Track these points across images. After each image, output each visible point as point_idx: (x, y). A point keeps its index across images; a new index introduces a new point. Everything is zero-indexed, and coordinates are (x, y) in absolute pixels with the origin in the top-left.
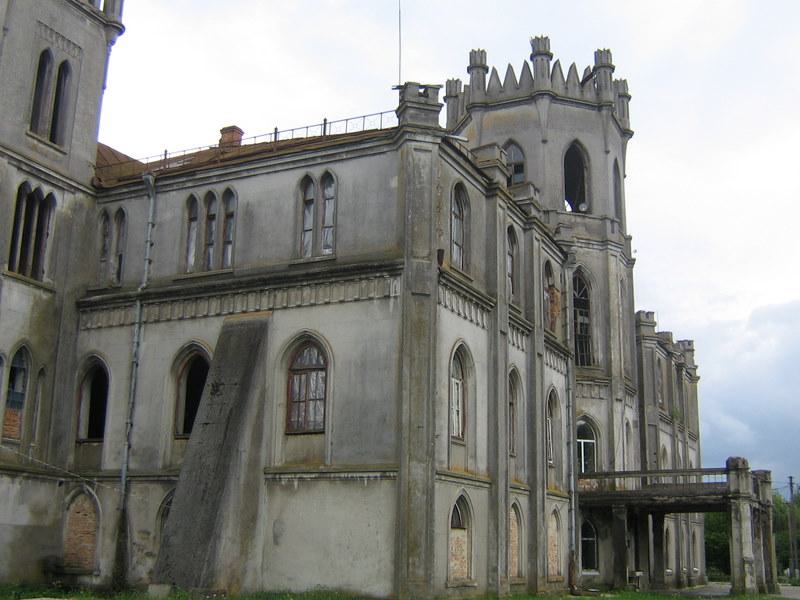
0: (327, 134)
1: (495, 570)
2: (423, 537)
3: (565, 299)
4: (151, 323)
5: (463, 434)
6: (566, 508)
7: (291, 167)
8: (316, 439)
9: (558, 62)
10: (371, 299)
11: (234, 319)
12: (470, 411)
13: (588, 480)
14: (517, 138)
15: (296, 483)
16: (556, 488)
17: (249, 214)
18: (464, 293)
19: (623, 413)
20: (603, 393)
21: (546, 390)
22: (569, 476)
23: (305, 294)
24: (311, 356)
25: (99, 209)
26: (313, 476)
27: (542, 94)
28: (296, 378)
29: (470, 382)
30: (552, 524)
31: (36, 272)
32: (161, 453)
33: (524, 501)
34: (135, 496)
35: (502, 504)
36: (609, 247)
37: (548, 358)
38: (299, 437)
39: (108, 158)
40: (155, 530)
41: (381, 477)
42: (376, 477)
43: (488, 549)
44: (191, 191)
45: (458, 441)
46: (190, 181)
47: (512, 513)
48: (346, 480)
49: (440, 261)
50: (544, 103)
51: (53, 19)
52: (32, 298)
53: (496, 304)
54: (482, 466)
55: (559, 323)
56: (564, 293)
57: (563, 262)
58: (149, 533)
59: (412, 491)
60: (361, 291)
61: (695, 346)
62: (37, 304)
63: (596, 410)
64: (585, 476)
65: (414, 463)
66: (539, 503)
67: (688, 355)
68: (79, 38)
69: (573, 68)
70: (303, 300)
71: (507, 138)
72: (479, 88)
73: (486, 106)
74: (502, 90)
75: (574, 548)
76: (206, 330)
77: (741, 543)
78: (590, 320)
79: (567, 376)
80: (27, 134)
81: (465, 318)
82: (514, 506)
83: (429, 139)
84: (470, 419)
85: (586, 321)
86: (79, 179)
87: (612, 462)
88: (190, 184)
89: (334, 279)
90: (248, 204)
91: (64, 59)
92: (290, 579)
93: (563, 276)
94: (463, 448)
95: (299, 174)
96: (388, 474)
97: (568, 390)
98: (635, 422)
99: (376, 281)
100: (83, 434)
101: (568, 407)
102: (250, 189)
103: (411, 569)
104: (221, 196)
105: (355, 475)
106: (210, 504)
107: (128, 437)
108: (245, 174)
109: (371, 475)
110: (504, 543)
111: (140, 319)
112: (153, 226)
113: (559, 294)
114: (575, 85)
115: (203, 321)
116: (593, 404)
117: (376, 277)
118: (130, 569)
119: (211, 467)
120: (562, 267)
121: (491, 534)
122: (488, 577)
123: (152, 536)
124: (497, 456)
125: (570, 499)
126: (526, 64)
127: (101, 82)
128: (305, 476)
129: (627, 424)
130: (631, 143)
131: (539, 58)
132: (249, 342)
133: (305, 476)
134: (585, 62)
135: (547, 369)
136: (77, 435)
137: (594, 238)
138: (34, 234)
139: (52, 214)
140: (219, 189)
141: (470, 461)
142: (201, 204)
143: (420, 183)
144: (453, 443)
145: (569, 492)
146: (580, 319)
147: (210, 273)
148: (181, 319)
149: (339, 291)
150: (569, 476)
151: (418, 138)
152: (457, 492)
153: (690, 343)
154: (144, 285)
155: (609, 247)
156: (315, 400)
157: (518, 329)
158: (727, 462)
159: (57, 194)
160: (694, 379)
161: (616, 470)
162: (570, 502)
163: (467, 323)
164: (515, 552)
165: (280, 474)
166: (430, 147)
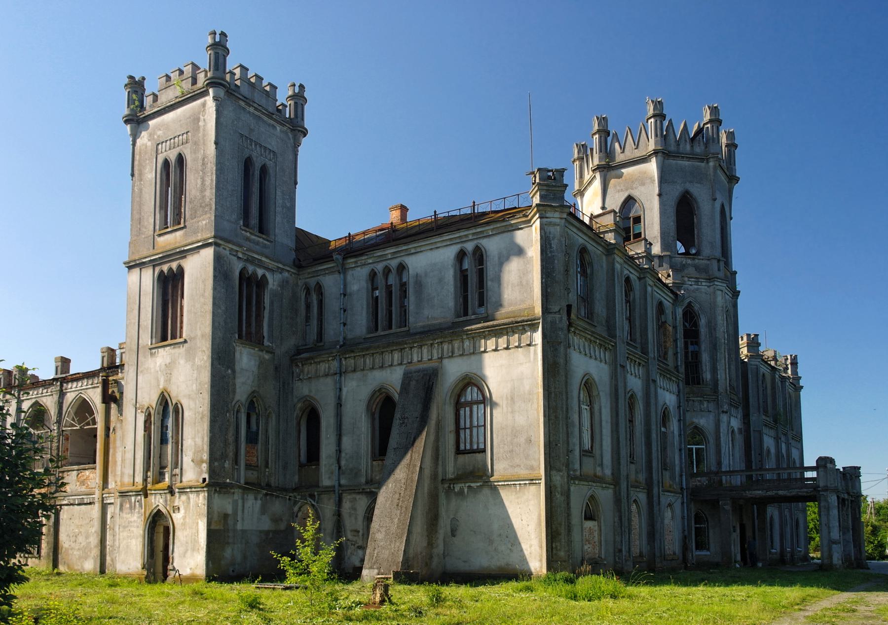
0: (476, 211)
1: (620, 551)
2: (563, 527)
3: (676, 333)
4: (349, 372)
5: (592, 447)
6: (679, 501)
11: (413, 368)
12: (597, 431)
19: (729, 423)
20: (712, 406)
21: (660, 408)
22: (681, 476)
23: (465, 346)
24: (471, 394)
25: (300, 283)
26: (478, 484)
28: (462, 412)
29: (596, 407)
30: (668, 514)
32: (363, 472)
33: (642, 497)
34: (346, 505)
35: (624, 501)
38: (466, 455)
39: (304, 239)
40: (363, 529)
43: (614, 535)
44: (372, 266)
45: (587, 453)
47: (634, 507)
51: (251, 130)
52: (258, 358)
53: (615, 343)
54: (608, 472)
55: (670, 353)
56: (675, 327)
57: (674, 301)
58: (358, 532)
59: (553, 493)
62: (262, 363)
63: (705, 422)
64: (698, 474)
66: (655, 499)
68: (273, 144)
70: (464, 349)
75: (686, 533)
77: (829, 527)
78: (700, 347)
79: (678, 396)
81: (591, 357)
82: (635, 501)
84: (597, 437)
87: (719, 464)
90: (417, 274)
92: (465, 562)
93: (674, 313)
94: (592, 459)
97: (679, 407)
98: (740, 430)
100: (303, 458)
101: (679, 420)
103: (554, 552)
104: (395, 269)
106: (404, 509)
107: (338, 461)
111: (340, 371)
112: (345, 295)
113: (671, 329)
115: (388, 371)
118: (346, 558)
119: (403, 481)
120: (673, 304)
121: (616, 524)
122: (615, 556)
123: (361, 534)
124: (619, 463)
125: (683, 495)
127: (293, 179)
129: (733, 431)
135: (660, 391)
136: (299, 461)
138: (254, 309)
139: (266, 291)
140: (394, 263)
141: (598, 469)
142: (380, 277)
145: (682, 489)
148: (373, 368)
150: (681, 476)
154: (342, 343)
156: (478, 426)
157: (635, 361)
158: (817, 461)
159: (269, 276)
161: (723, 470)
162: (683, 497)
163: (593, 361)
164: (637, 537)
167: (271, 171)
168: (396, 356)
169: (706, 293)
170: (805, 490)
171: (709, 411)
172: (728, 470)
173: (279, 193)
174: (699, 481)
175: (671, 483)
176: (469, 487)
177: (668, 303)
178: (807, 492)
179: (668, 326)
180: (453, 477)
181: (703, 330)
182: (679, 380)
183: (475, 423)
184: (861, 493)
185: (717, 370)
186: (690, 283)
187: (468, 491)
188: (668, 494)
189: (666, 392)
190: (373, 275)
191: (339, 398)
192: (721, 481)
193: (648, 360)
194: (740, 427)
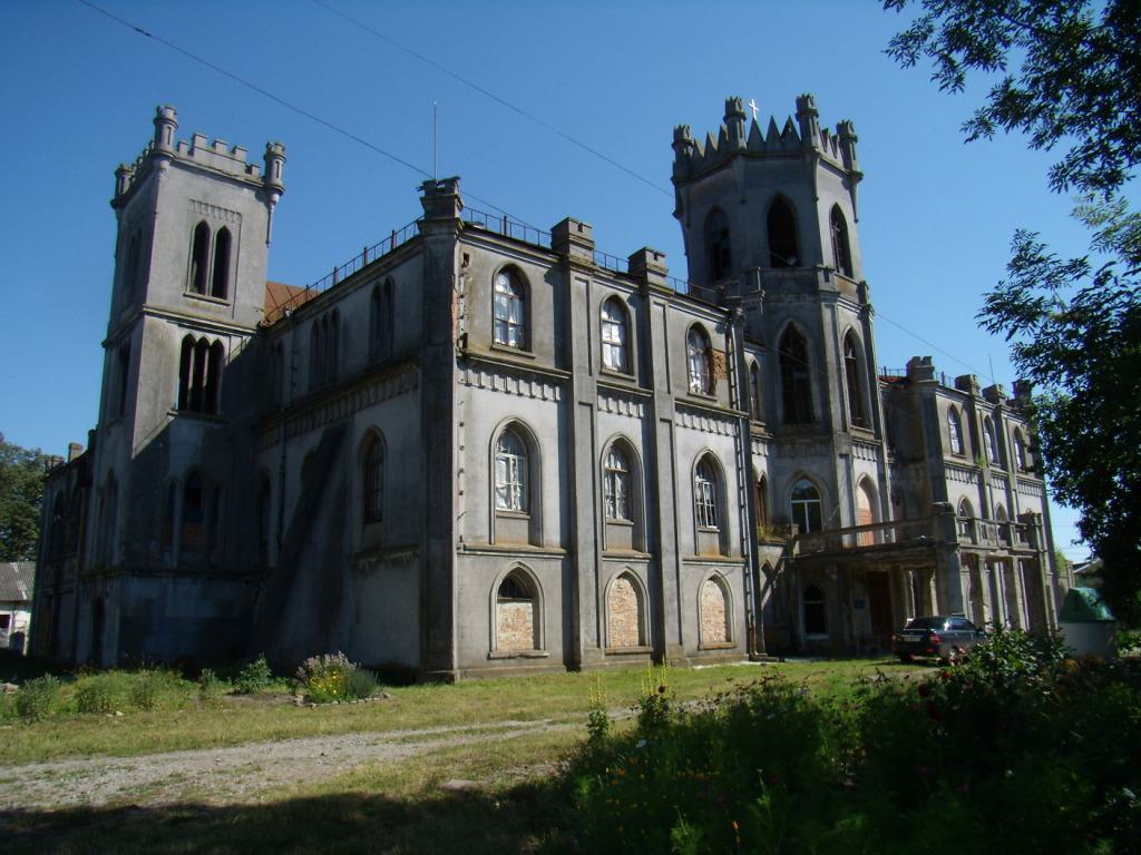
9: (754, 122)
10: (407, 391)
19: (849, 468)
27: (735, 155)
31: (211, 408)
33: (642, 571)
37: (678, 418)
48: (395, 562)
49: (465, 345)
50: (738, 165)
53: (571, 376)
69: (773, 125)
76: (314, 439)
80: (185, 295)
85: (804, 376)
86: (246, 324)
91: (222, 226)
126: (722, 132)
132: (336, 439)
134: (785, 113)
140: (330, 311)
144: (498, 517)
146: (797, 375)
152: (507, 566)
159: (224, 340)
167: (234, 234)
173: (242, 254)
186: (788, 300)
190: (315, 326)
191: (283, 467)
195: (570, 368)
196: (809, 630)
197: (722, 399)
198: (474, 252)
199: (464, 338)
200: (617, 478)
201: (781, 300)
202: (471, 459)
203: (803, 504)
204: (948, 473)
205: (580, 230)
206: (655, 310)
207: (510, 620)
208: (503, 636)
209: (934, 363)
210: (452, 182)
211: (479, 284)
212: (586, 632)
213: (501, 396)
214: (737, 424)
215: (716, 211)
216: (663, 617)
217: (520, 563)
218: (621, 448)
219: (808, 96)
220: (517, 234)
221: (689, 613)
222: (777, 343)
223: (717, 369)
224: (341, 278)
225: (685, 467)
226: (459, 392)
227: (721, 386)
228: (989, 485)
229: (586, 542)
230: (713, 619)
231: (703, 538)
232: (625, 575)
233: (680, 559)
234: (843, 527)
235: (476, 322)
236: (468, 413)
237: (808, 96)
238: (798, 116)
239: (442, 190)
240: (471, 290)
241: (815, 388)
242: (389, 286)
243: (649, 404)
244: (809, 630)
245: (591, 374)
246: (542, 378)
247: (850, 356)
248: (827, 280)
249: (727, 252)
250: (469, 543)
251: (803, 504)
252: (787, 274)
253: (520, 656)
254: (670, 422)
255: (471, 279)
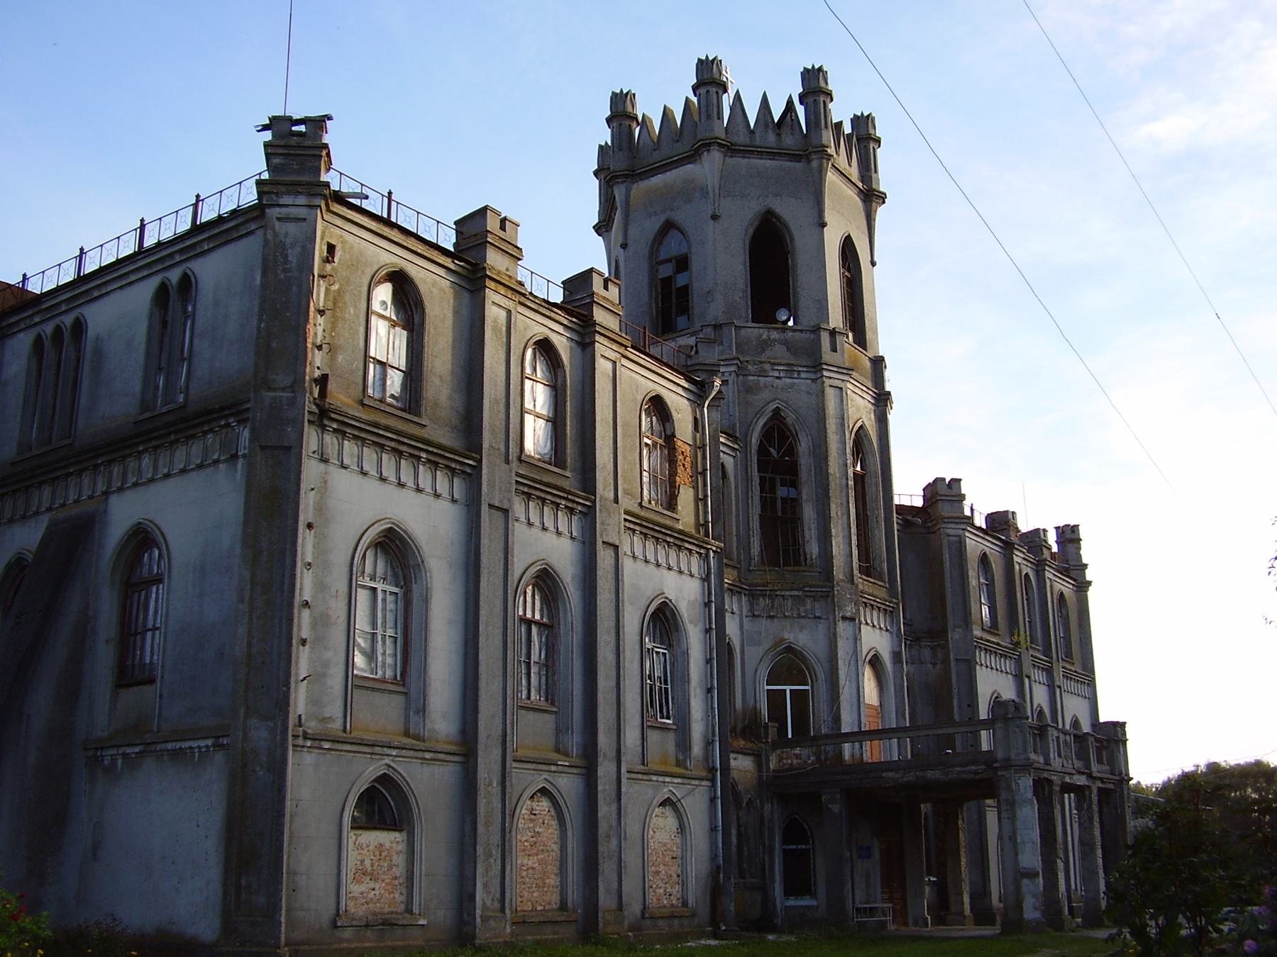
1: (472, 897)
7: (145, 273)
8: (147, 689)
9: (738, 96)
10: (216, 462)
13: (797, 751)
14: (679, 217)
15: (120, 762)
16: (679, 763)
17: (99, 354)
18: (393, 444)
19: (856, 639)
20: (819, 608)
26: (137, 749)
27: (707, 145)
33: (568, 785)
36: (825, 373)
37: (631, 544)
41: (214, 745)
42: (207, 747)
46: (37, 313)
48: (176, 755)
49: (323, 394)
60: (205, 454)
61: (1083, 534)
65: (254, 722)
67: (1070, 547)
69: (765, 100)
71: (662, 219)
72: (620, 150)
73: (633, 175)
74: (658, 144)
78: (799, 493)
83: (302, 200)
85: (793, 493)
87: (837, 719)
88: (37, 319)
89: (173, 437)
94: (401, 699)
95: (154, 282)
96: (221, 740)
97: (707, 605)
98: (896, 657)
99: (224, 431)
101: (708, 631)
102: (99, 317)
105: (187, 744)
108: (96, 294)
109: (202, 743)
110: (496, 853)
114: (766, 125)
116: (801, 629)
117: (222, 427)
125: (713, 780)
128: (128, 750)
130: (882, 214)
131: (702, 91)
133: (128, 750)
135: (628, 565)
137: (804, 363)
140: (68, 320)
142: (48, 344)
143: (285, 271)
146: (782, 492)
147: (49, 448)
149: (180, 457)
151: (281, 201)
152: (369, 770)
153: (1074, 529)
155: (825, 373)
160: (1082, 586)
161: (845, 729)
163: (408, 495)
165: (102, 748)
166: (302, 212)
168: (47, 492)
169: (809, 393)
170: (973, 767)
171: (816, 618)
172: (856, 730)
174: (797, 756)
175: (681, 757)
176: (125, 755)
177: (679, 397)
178: (976, 773)
179: (679, 443)
180: (105, 734)
181: (805, 462)
182: (708, 549)
183: (150, 626)
184: (1127, 774)
185: (831, 536)
187: (122, 763)
188: (661, 779)
189: (665, 572)
190: (38, 343)
192: (840, 754)
193: (594, 502)
194: (897, 649)
195: (478, 449)
196: (788, 892)
197: (685, 514)
198: (344, 242)
199: (323, 381)
200: (534, 630)
201: (763, 374)
202: (321, 586)
203: (785, 690)
204: (981, 657)
205: (503, 228)
206: (603, 367)
207: (368, 862)
208: (356, 889)
209: (965, 488)
210: (318, 123)
211: (347, 297)
212: (485, 885)
213: (372, 485)
214: (707, 555)
215: (669, 226)
216: (597, 863)
217: (389, 766)
218: (546, 581)
219: (820, 69)
220: (403, 218)
221: (631, 858)
222: (755, 440)
223: (680, 470)
224: (90, 267)
225: (632, 621)
226: (311, 470)
227: (686, 497)
228: (1029, 677)
229: (488, 736)
230: (662, 868)
231: (653, 736)
232: (544, 791)
233: (623, 770)
234: (843, 732)
235: (340, 358)
236: (320, 508)
237: (820, 69)
238: (802, 98)
239: (300, 134)
240: (335, 302)
241: (809, 512)
242: (187, 283)
243: (589, 514)
244: (788, 892)
245: (507, 461)
246: (437, 458)
247: (858, 468)
248: (834, 350)
249: (685, 291)
250: (312, 726)
251: (785, 690)
252: (775, 335)
253: (383, 924)
254: (616, 548)
255: (336, 287)
